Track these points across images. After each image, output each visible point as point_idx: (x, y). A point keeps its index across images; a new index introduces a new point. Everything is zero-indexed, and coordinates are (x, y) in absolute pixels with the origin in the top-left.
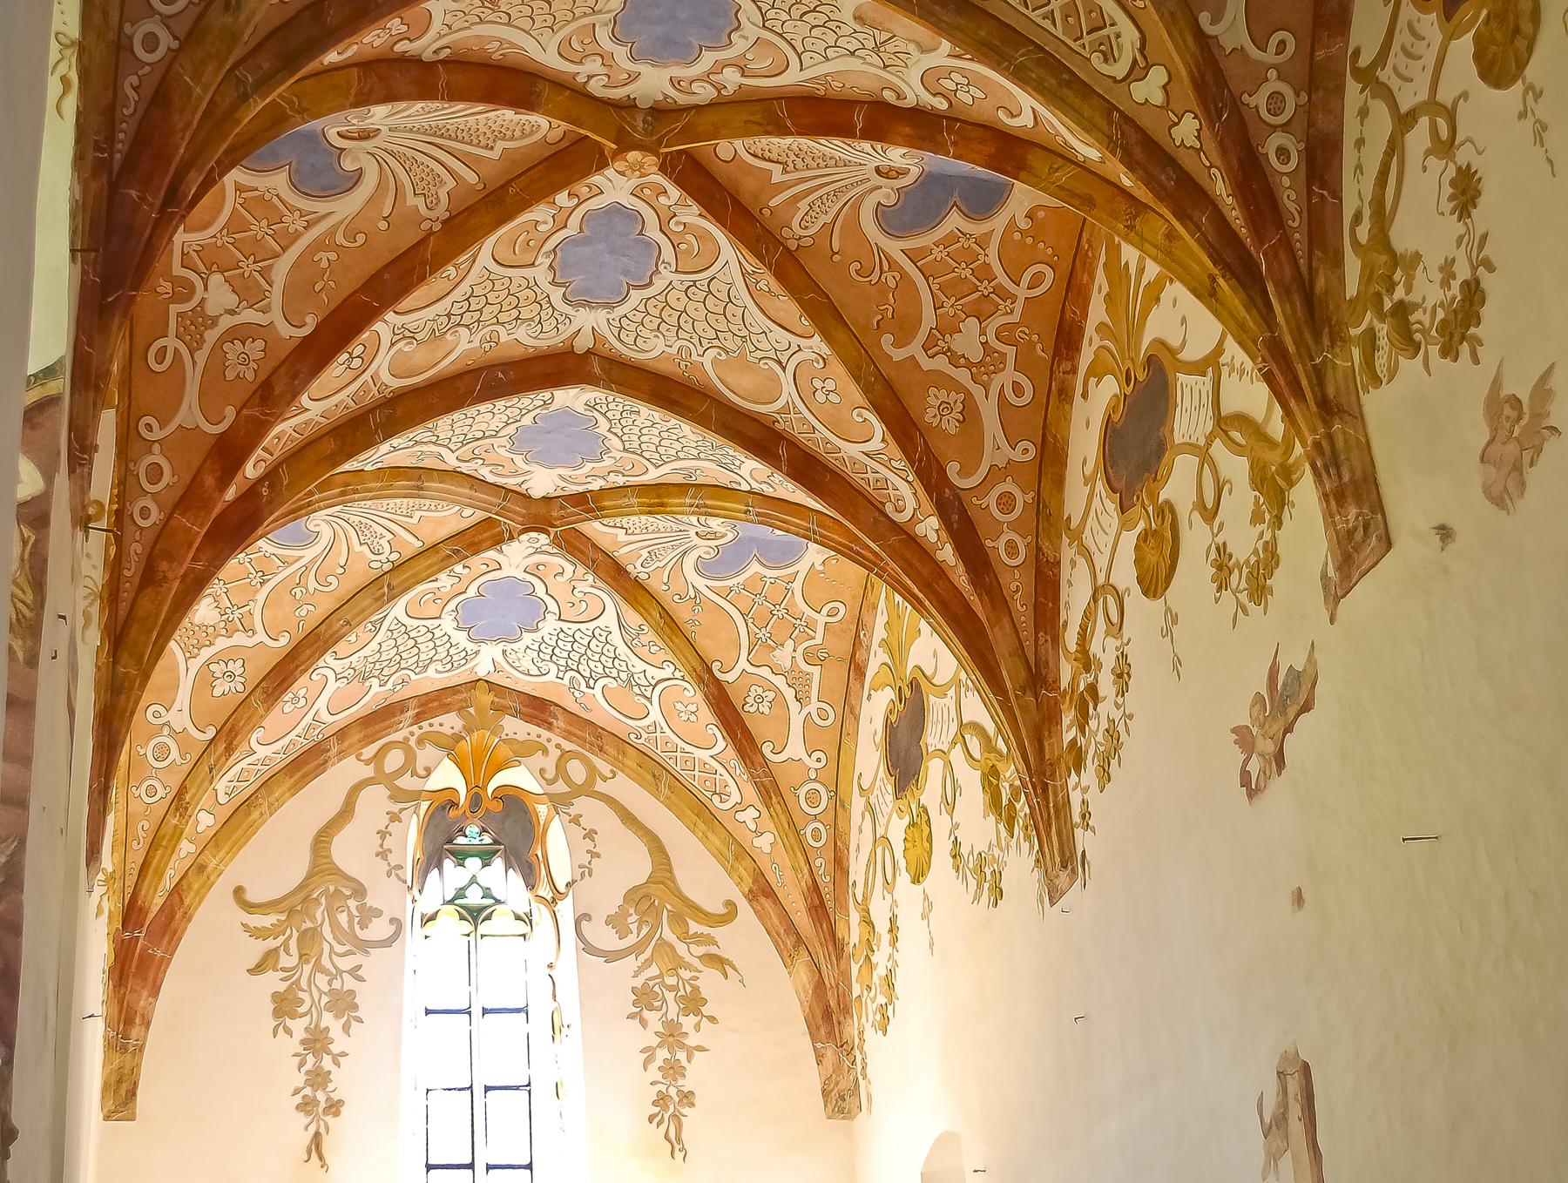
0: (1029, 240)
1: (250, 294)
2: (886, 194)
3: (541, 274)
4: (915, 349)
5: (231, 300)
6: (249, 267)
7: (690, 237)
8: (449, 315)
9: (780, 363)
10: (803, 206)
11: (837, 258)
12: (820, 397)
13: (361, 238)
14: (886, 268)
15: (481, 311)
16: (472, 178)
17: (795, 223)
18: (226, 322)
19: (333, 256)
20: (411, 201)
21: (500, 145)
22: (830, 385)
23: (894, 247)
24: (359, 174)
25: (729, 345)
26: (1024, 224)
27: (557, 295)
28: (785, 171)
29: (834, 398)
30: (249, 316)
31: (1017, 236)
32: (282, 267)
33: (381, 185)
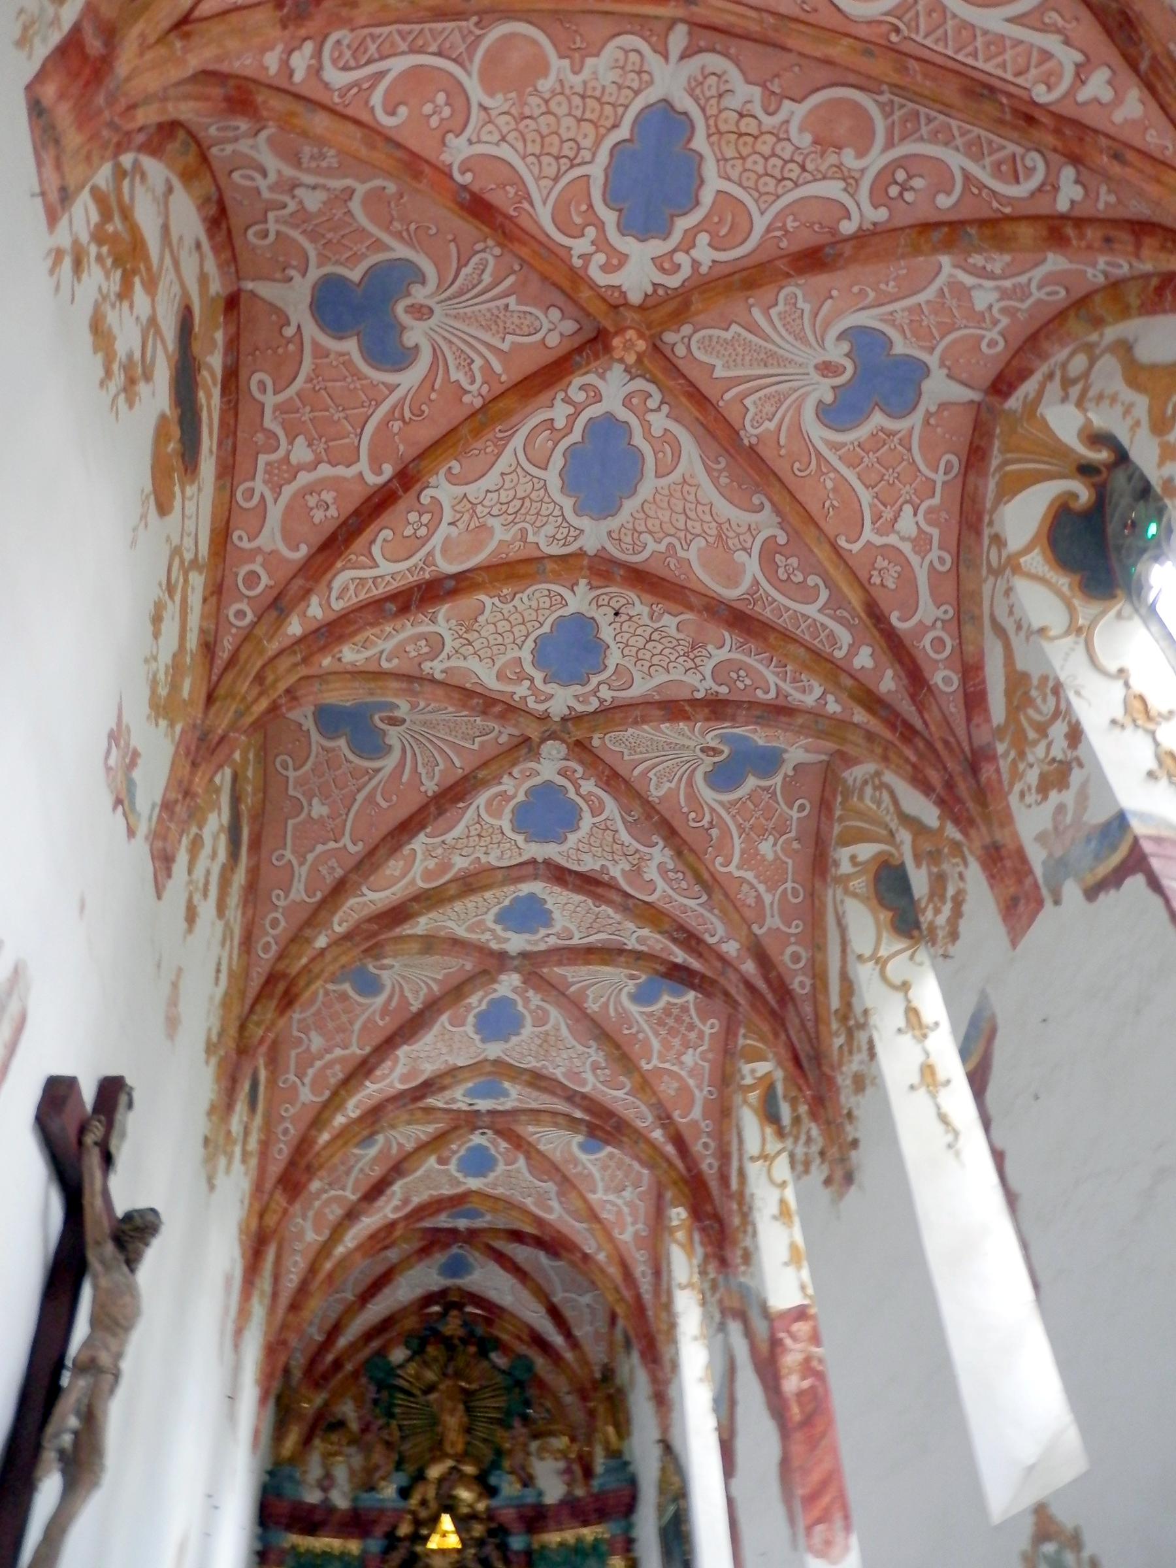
0: (281, 259)
1: (962, 292)
2: (420, 294)
3: (713, 183)
4: (361, 189)
5: (975, 294)
6: (952, 302)
7: (578, 220)
8: (803, 168)
9: (485, 109)
10: (487, 278)
11: (450, 237)
12: (441, 98)
13: (856, 289)
14: (405, 234)
15: (774, 155)
16: (757, 313)
17: (491, 262)
18: (989, 284)
19: (882, 286)
20: (807, 308)
21: (728, 335)
22: (434, 122)
23: (401, 251)
24: (841, 336)
25: (534, 101)
26: (292, 272)
27: (699, 142)
28: (507, 306)
29: (428, 108)
30: (968, 280)
31: (294, 263)
32: (930, 293)
33: (827, 325)
